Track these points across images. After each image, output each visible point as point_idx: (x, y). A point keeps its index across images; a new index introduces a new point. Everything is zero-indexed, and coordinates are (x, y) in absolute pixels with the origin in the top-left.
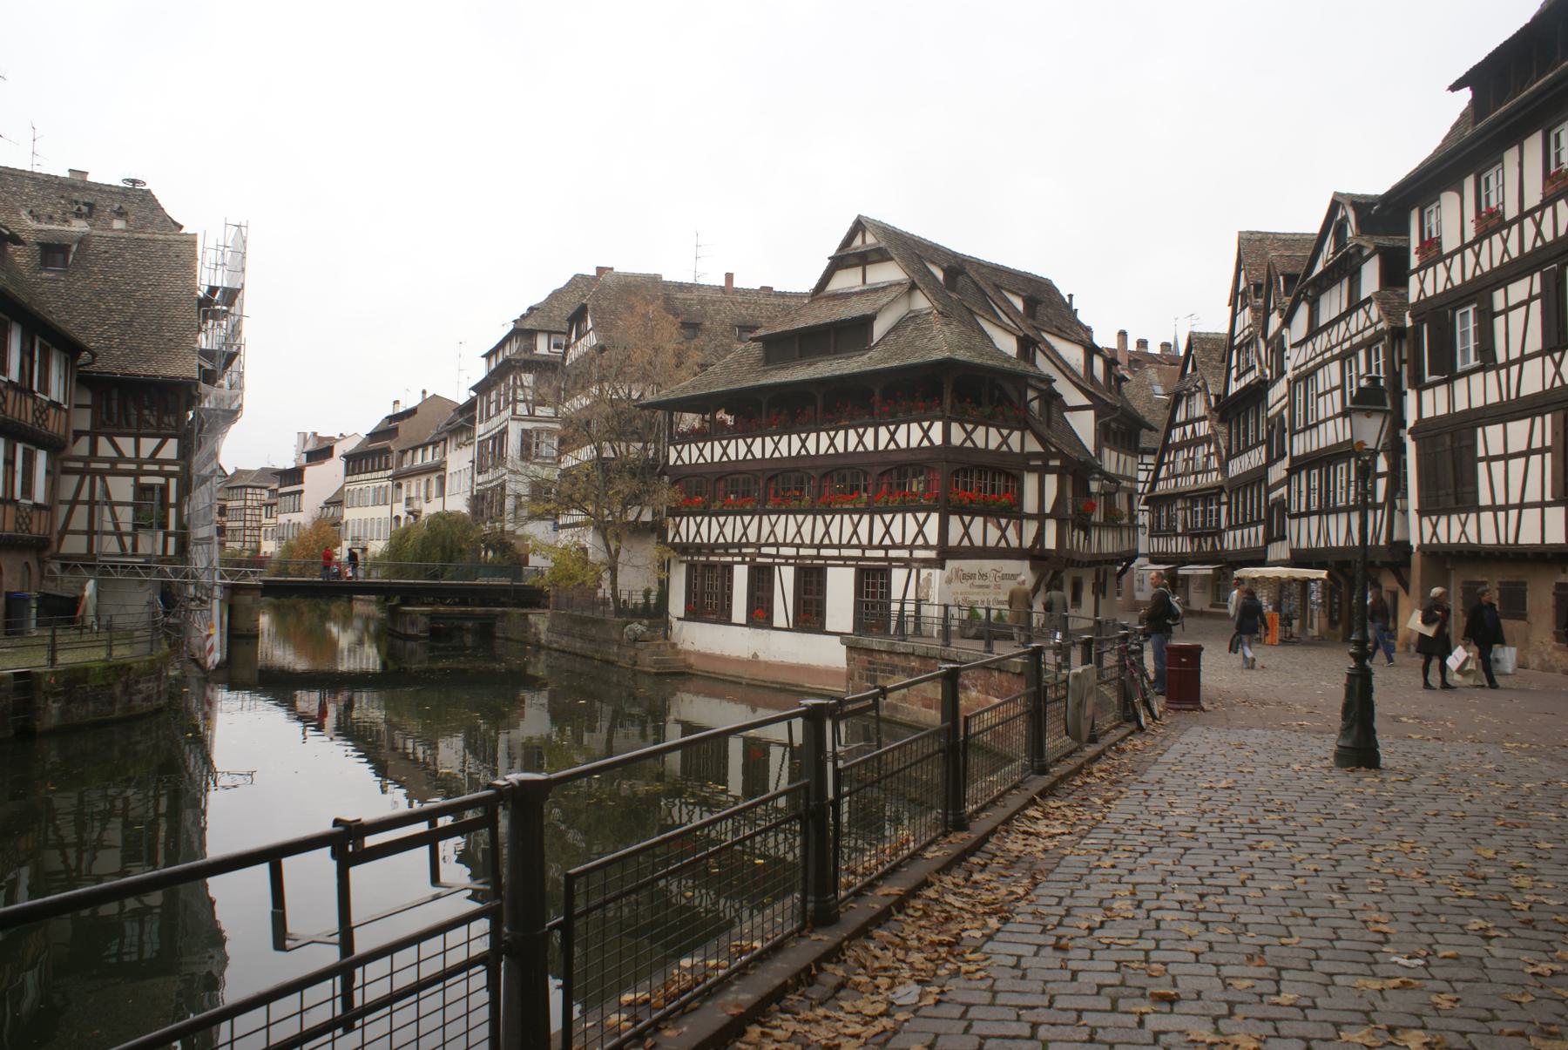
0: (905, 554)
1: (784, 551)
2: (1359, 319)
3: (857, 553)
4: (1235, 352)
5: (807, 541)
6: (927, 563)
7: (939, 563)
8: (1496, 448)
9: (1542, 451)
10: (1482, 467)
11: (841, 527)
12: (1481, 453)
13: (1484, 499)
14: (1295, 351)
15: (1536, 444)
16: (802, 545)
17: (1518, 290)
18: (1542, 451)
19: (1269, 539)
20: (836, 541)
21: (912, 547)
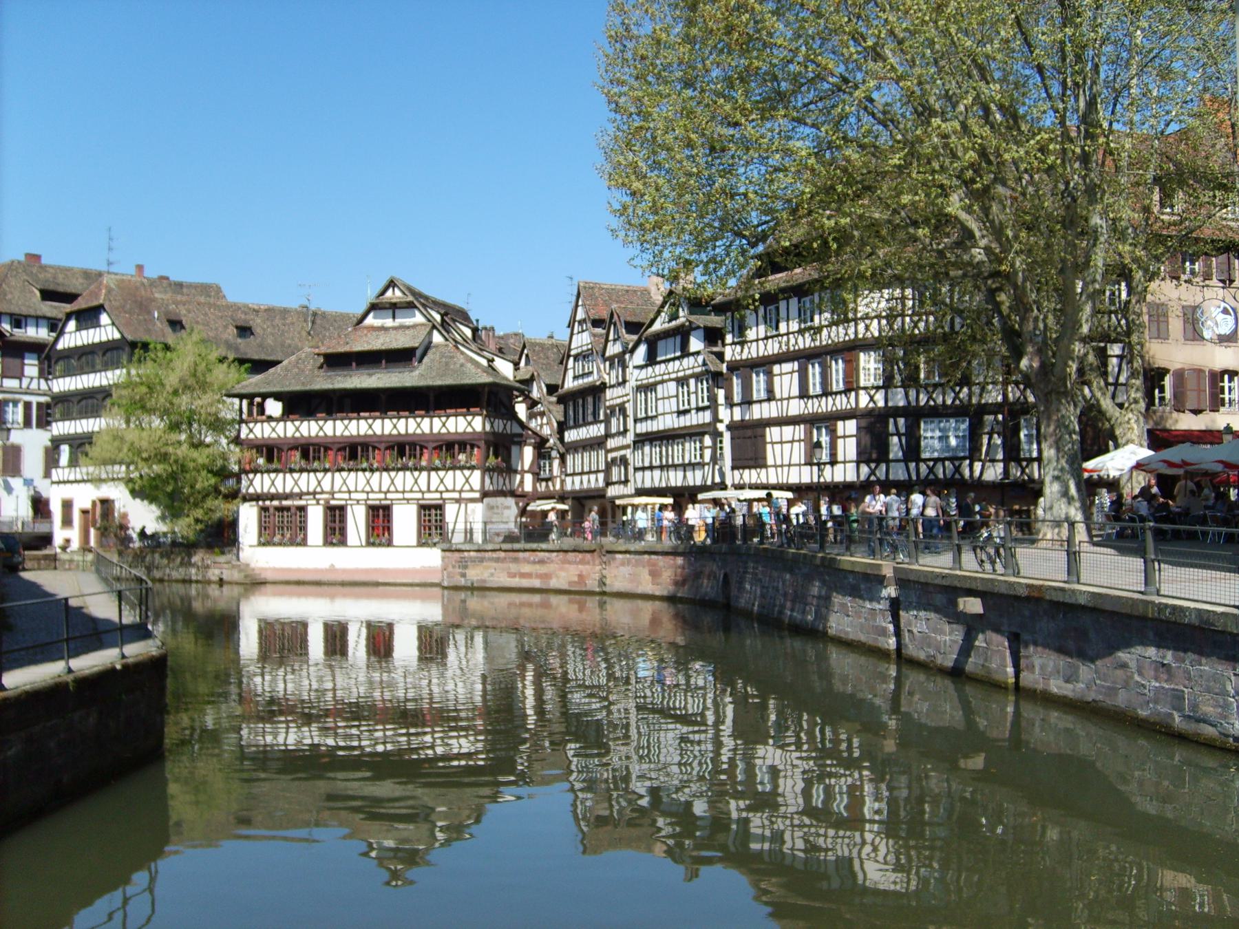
0: (456, 495)
1: (354, 496)
2: (688, 362)
3: (419, 496)
4: (571, 359)
5: (376, 488)
6: (473, 500)
7: (481, 500)
8: (776, 438)
9: (799, 441)
10: (769, 447)
11: (404, 480)
12: (768, 439)
13: (770, 461)
14: (636, 372)
15: (797, 438)
16: (372, 491)
17: (787, 367)
18: (799, 441)
19: (608, 483)
20: (400, 489)
21: (461, 491)
